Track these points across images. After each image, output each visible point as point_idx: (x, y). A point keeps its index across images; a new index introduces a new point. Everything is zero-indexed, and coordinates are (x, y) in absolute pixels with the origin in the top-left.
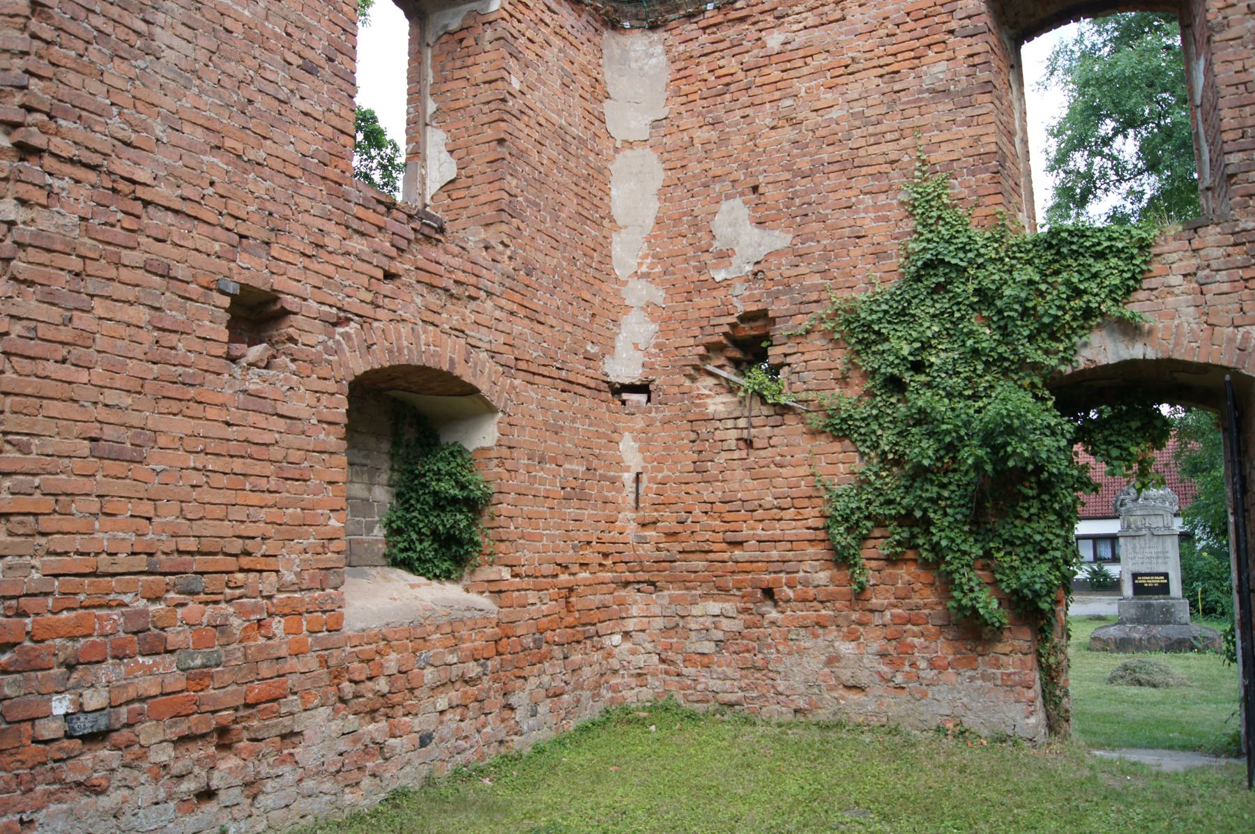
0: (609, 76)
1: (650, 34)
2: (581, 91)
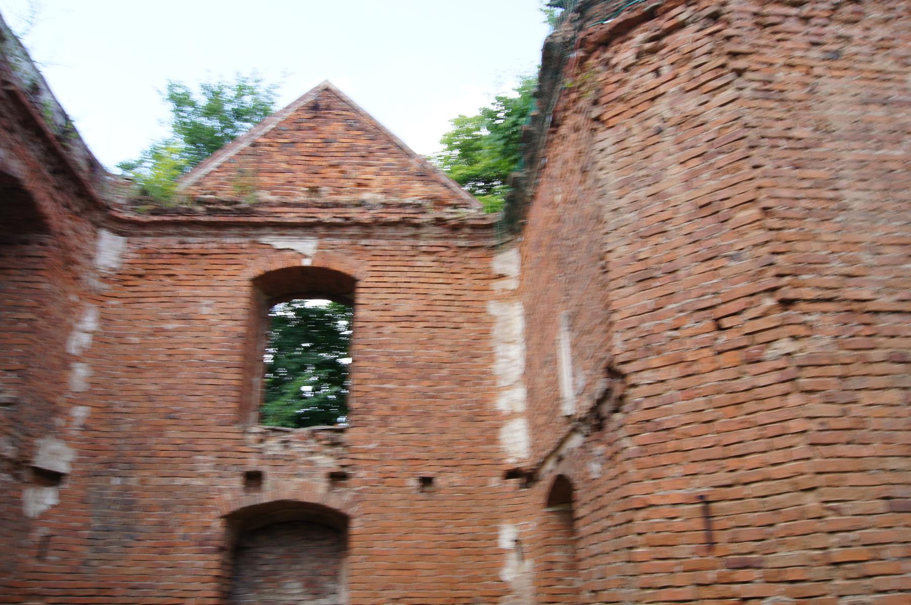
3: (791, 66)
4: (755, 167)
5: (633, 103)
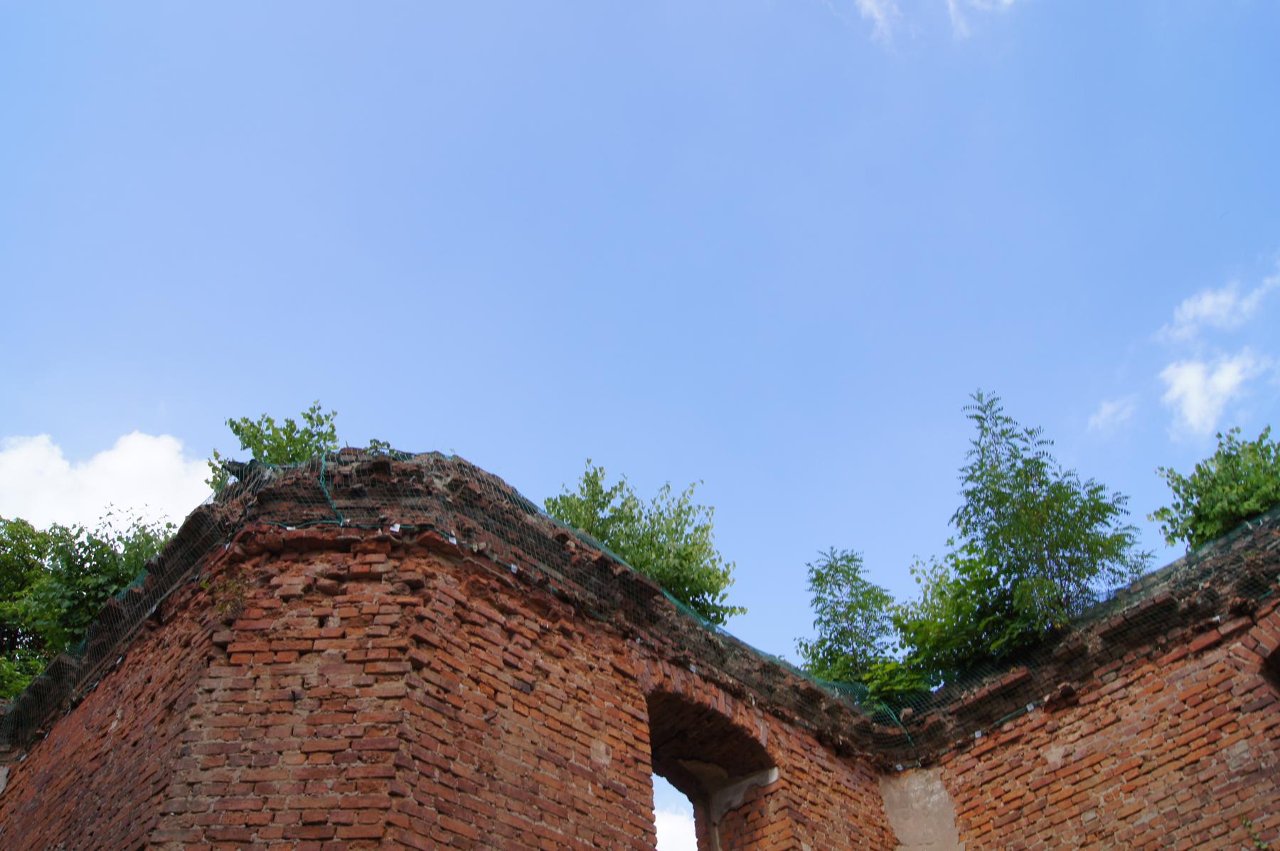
0: (894, 820)
1: (925, 771)
2: (870, 844)
3: (477, 681)
4: (393, 794)
5: (275, 645)
